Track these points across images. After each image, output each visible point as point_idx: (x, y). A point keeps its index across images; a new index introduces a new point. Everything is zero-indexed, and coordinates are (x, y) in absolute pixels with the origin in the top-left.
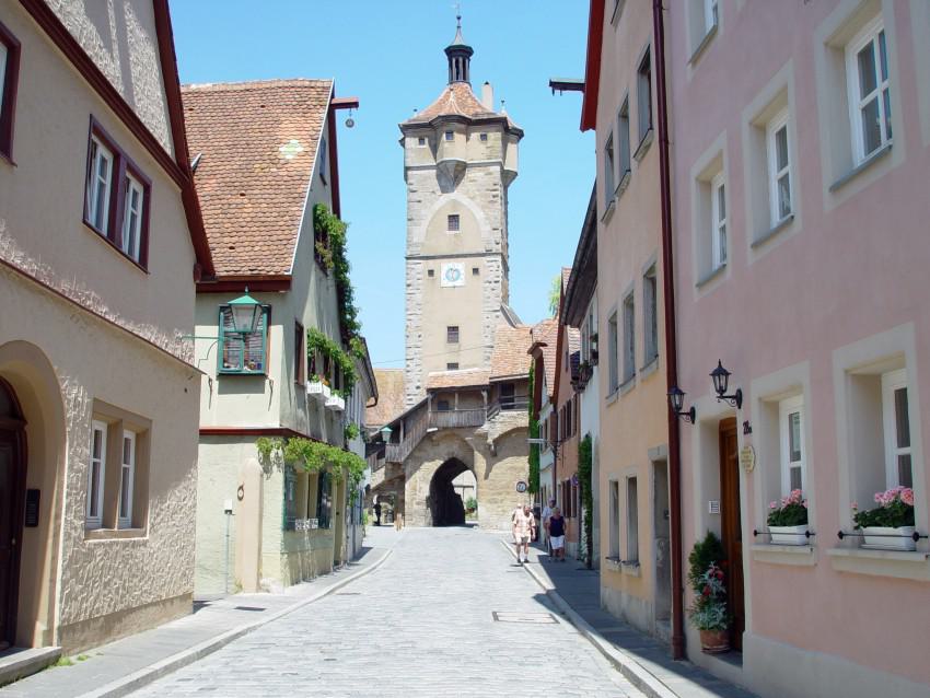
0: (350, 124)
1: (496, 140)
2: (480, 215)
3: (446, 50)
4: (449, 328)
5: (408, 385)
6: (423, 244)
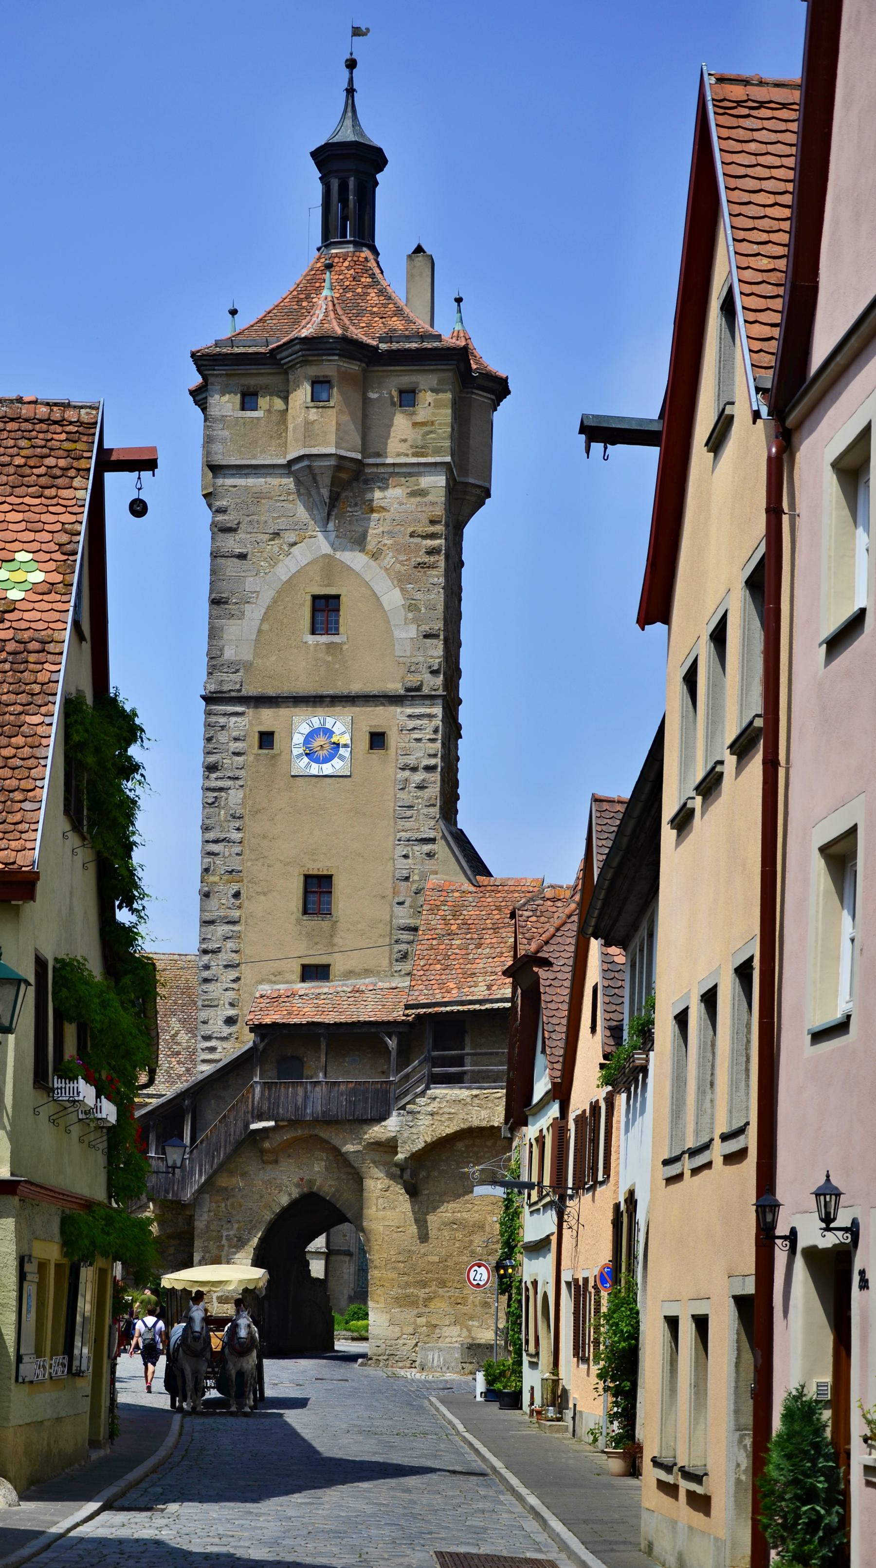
0: (138, 508)
1: (438, 405)
2: (392, 598)
3: (314, 154)
4: (308, 878)
5: (203, 1015)
6: (248, 666)
